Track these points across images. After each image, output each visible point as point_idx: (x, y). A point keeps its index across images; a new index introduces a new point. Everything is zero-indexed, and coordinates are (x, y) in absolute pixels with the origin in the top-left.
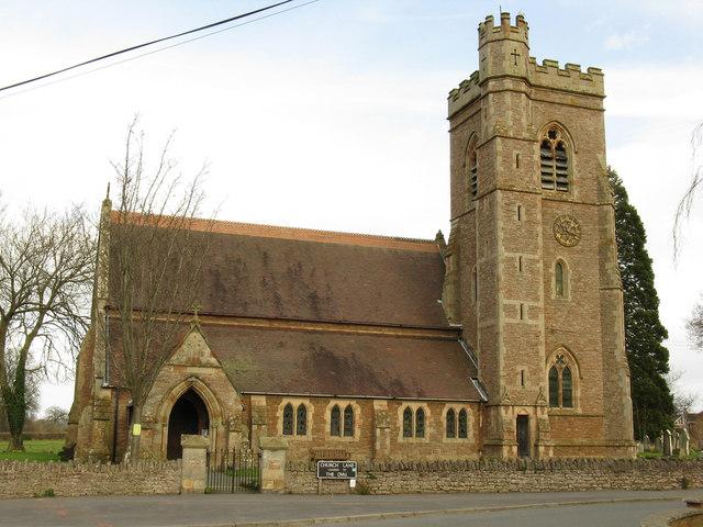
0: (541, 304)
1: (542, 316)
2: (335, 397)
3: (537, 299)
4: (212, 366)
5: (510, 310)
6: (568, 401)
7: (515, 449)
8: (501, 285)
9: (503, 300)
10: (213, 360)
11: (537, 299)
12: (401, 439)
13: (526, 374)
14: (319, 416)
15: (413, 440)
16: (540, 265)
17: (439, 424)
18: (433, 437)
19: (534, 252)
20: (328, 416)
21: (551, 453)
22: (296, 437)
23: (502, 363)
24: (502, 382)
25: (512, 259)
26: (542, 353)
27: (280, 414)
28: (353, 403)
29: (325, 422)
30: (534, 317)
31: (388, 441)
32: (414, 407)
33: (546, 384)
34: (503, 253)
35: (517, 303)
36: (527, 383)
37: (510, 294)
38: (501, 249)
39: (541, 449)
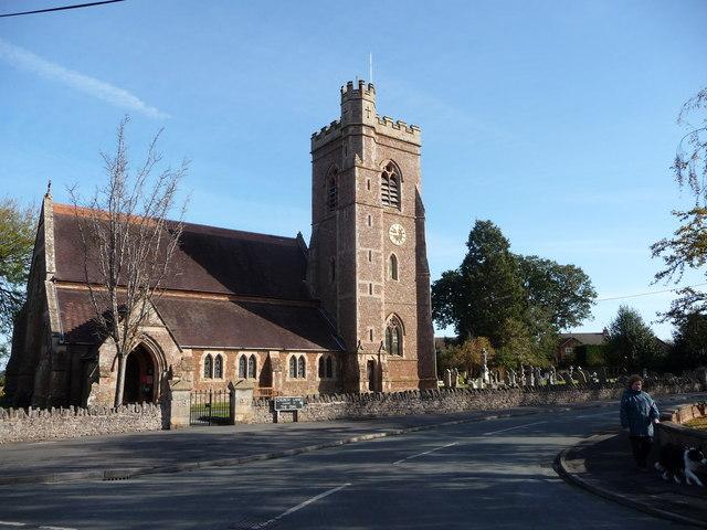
0: (382, 284)
1: (383, 292)
2: (243, 350)
3: (380, 280)
4: (158, 326)
5: (363, 287)
6: (399, 352)
7: (367, 384)
8: (357, 270)
9: (359, 281)
10: (159, 321)
11: (380, 280)
12: (288, 380)
13: (374, 332)
14: (231, 363)
15: (299, 379)
16: (382, 257)
17: (314, 368)
18: (311, 378)
19: (378, 247)
20: (237, 363)
21: (390, 386)
22: (215, 380)
23: (358, 325)
24: (358, 338)
25: (364, 252)
26: (383, 317)
27: (202, 362)
28: (255, 353)
29: (234, 368)
30: (378, 292)
31: (281, 381)
32: (298, 355)
33: (384, 339)
34: (359, 248)
35: (368, 283)
36: (374, 338)
37: (363, 277)
38: (358, 244)
39: (384, 383)
